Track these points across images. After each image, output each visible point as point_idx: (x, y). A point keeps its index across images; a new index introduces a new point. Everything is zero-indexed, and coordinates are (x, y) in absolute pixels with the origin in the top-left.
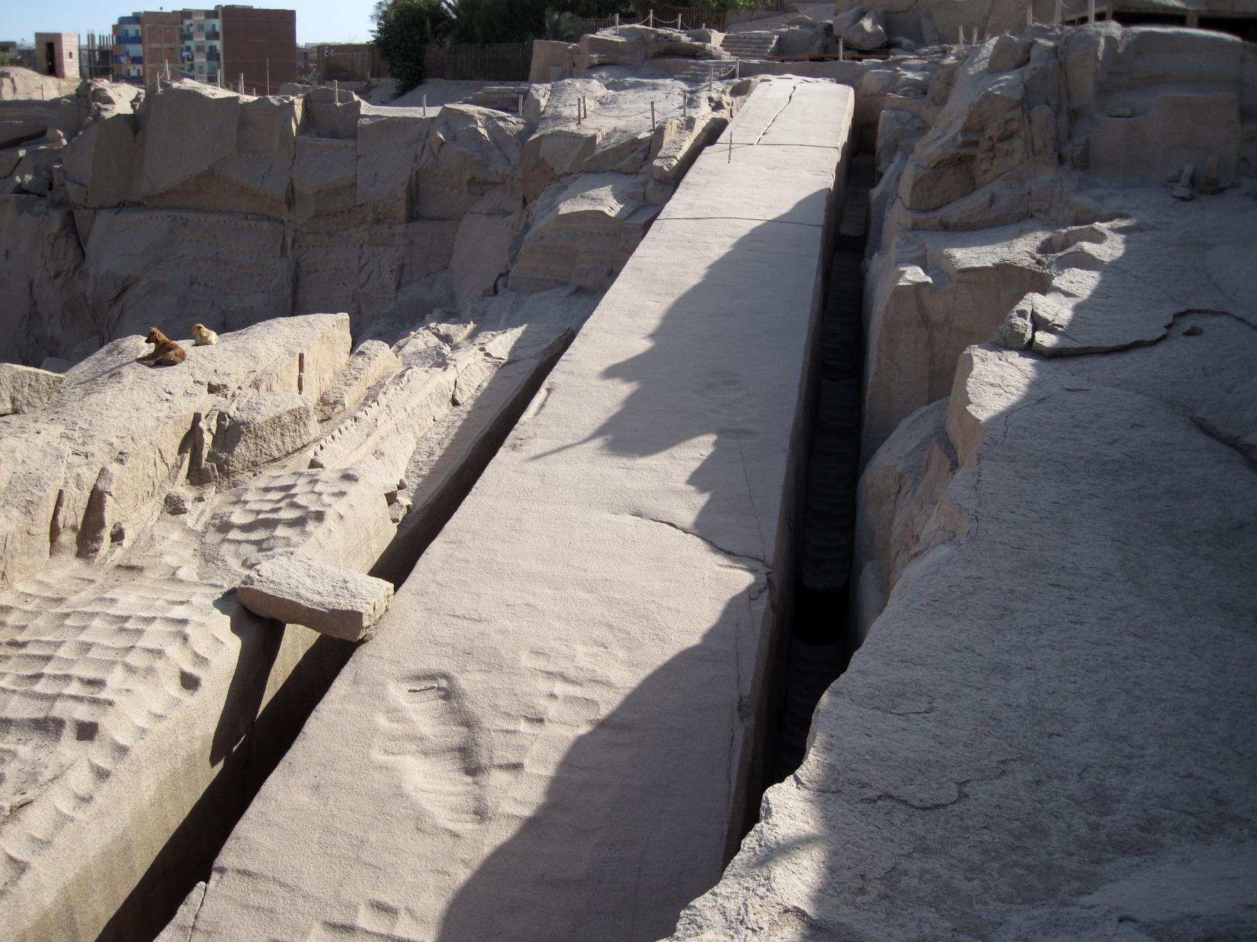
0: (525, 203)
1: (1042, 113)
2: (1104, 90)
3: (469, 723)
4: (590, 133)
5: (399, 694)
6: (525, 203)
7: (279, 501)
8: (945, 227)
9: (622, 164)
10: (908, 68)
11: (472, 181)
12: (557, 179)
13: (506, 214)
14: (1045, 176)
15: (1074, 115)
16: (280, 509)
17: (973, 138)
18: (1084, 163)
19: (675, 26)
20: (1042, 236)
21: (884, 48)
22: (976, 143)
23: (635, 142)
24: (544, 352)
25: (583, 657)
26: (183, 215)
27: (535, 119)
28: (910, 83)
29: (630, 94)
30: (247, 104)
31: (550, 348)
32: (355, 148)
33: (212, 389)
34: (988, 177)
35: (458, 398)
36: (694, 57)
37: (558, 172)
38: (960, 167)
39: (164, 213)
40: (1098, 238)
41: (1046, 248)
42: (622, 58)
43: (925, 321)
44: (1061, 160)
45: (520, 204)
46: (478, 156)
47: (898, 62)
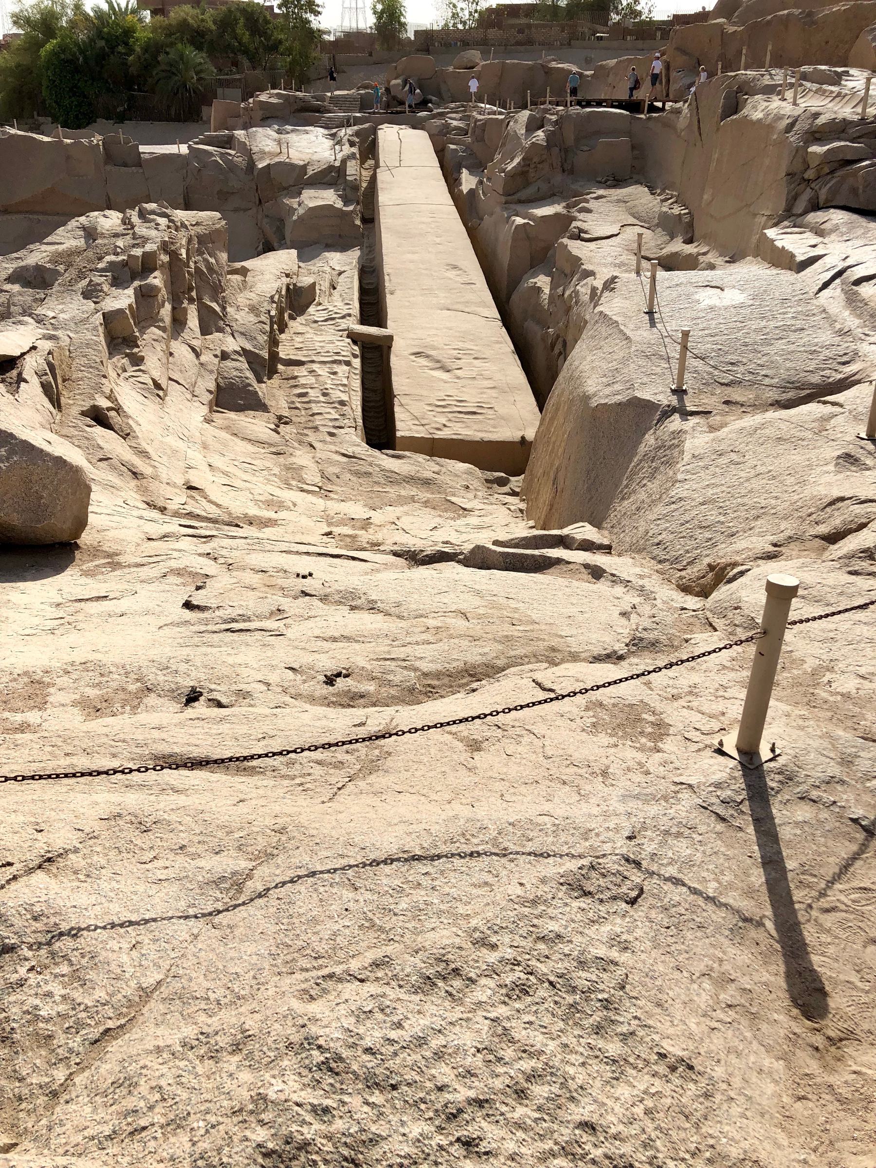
1: (555, 150)
2: (577, 140)
3: (438, 361)
4: (302, 163)
5: (413, 357)
8: (520, 202)
9: (325, 180)
11: (220, 192)
13: (245, 210)
14: (558, 178)
15: (566, 151)
18: (572, 172)
20: (564, 204)
21: (423, 104)
23: (331, 168)
25: (461, 345)
26: (36, 217)
27: (248, 153)
28: (457, 128)
29: (293, 138)
30: (68, 145)
33: (287, 276)
36: (318, 112)
37: (284, 185)
38: (521, 176)
39: (22, 216)
40: (587, 201)
41: (568, 207)
43: (528, 238)
44: (564, 171)
46: (222, 177)
47: (442, 115)
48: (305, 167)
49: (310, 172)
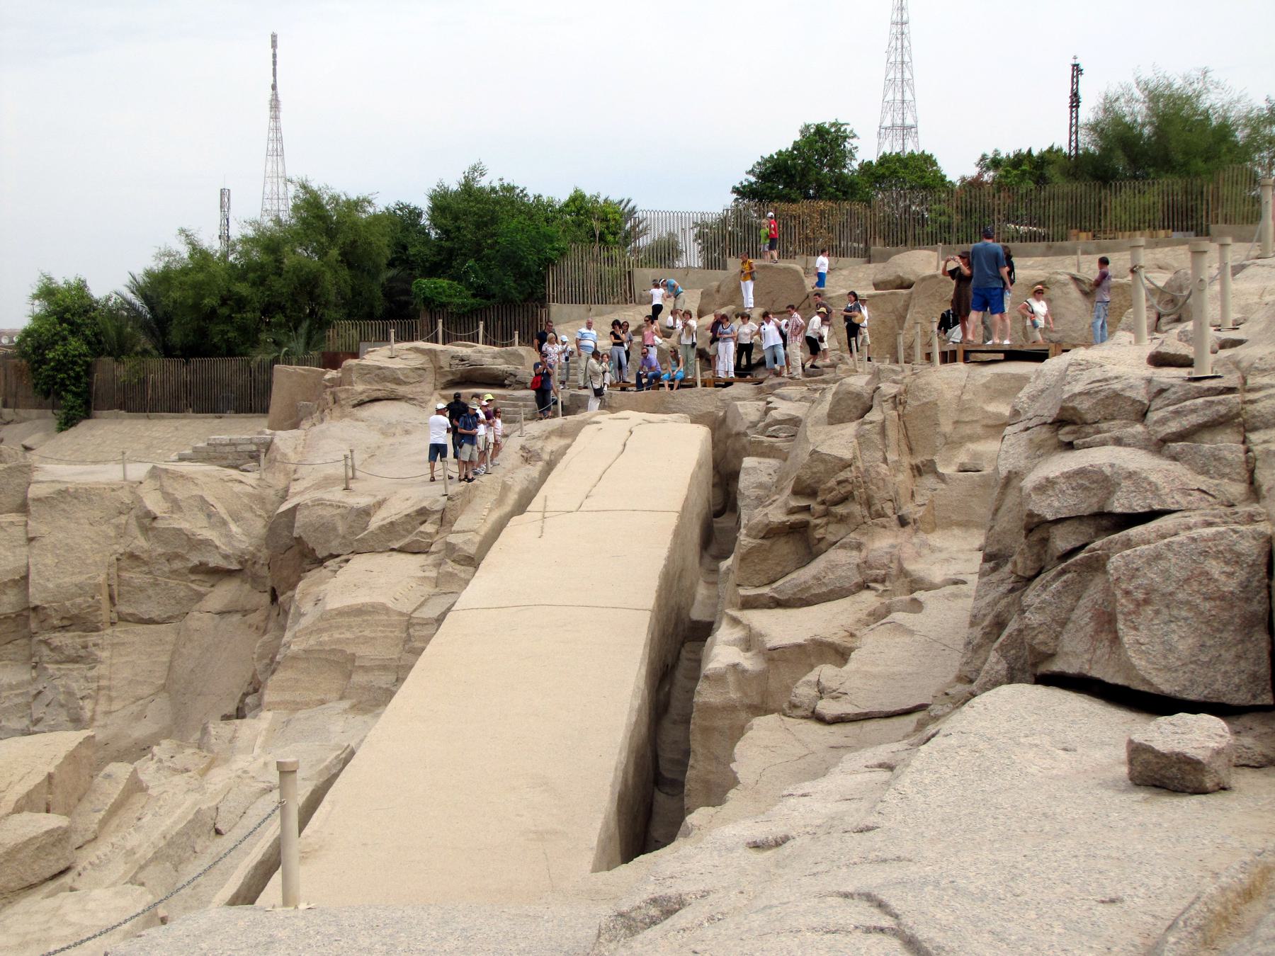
0: (274, 598)
6: (274, 598)
7: (48, 922)
10: (783, 398)
12: (320, 562)
16: (50, 928)
17: (804, 503)
19: (475, 339)
22: (807, 509)
24: (320, 773)
31: (327, 768)
32: (26, 525)
34: (823, 545)
35: (219, 826)
37: (321, 553)
42: (401, 390)
45: (266, 598)
48: (366, 513)
49: (376, 522)
